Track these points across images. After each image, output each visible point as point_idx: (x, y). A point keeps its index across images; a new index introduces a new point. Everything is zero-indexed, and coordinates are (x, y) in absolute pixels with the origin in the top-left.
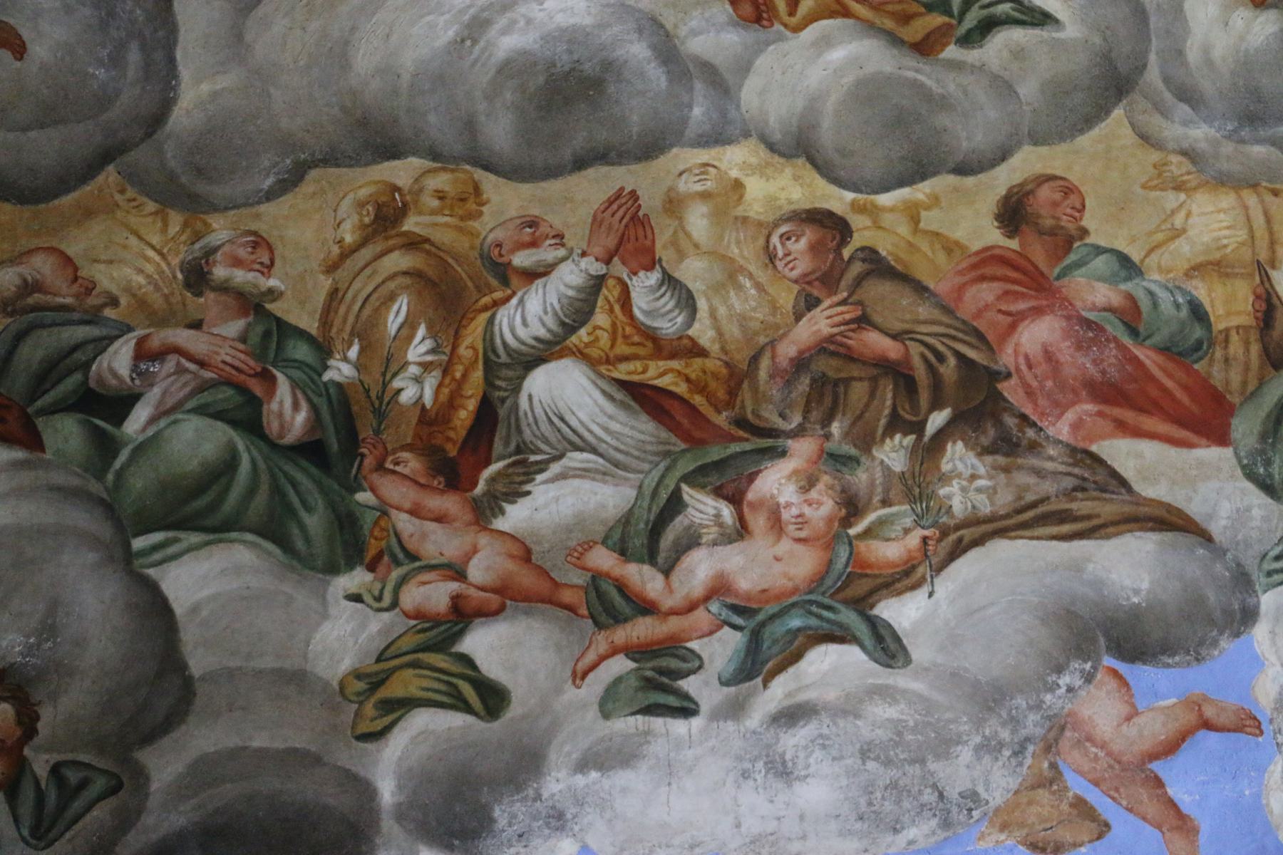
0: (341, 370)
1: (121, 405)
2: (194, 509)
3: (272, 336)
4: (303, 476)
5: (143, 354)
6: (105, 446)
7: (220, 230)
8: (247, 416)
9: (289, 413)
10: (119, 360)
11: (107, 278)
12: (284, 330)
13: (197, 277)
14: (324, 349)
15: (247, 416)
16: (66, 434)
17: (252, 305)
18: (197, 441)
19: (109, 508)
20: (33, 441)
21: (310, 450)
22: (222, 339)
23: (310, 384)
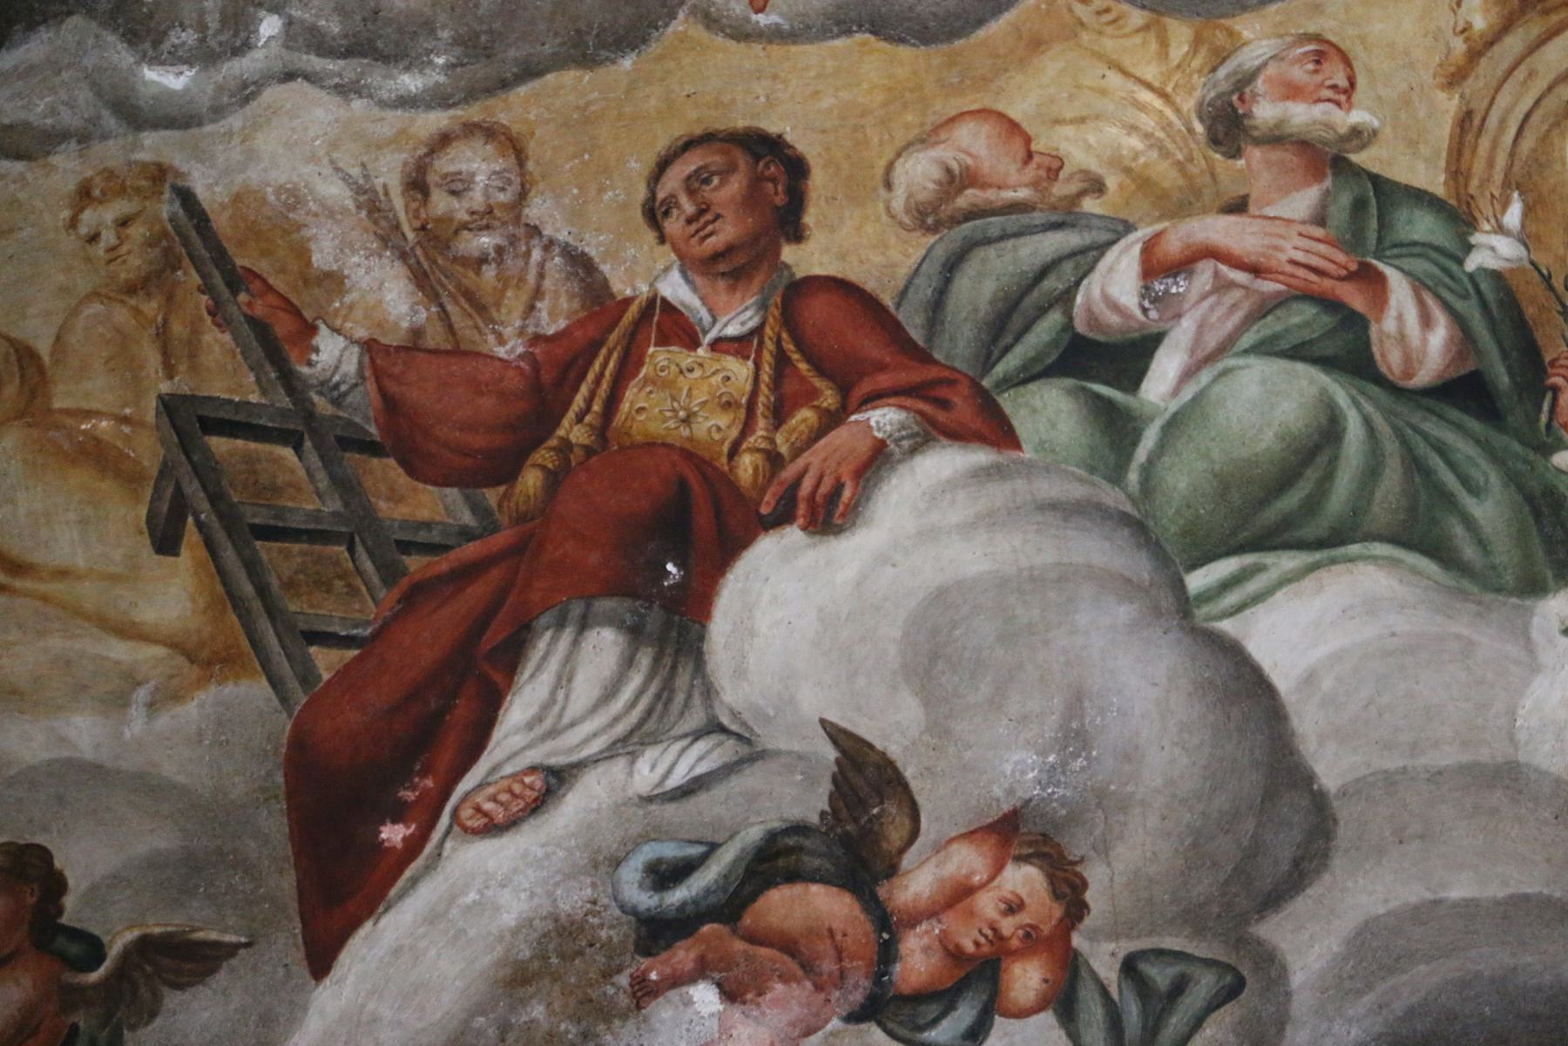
0: (1495, 250)
1: (1127, 357)
2: (1280, 512)
3: (1368, 203)
4: (1458, 438)
5: (1155, 267)
6: (1116, 428)
7: (1256, 38)
8: (1347, 350)
9: (1416, 334)
10: (1116, 284)
11: (1080, 148)
12: (1385, 194)
13: (1228, 126)
14: (1461, 218)
15: (1347, 350)
16: (1049, 414)
17: (1328, 159)
18: (1267, 401)
19: (1139, 529)
20: (998, 432)
21: (1463, 391)
22: (1285, 222)
23: (1444, 278)
